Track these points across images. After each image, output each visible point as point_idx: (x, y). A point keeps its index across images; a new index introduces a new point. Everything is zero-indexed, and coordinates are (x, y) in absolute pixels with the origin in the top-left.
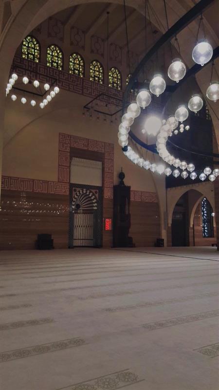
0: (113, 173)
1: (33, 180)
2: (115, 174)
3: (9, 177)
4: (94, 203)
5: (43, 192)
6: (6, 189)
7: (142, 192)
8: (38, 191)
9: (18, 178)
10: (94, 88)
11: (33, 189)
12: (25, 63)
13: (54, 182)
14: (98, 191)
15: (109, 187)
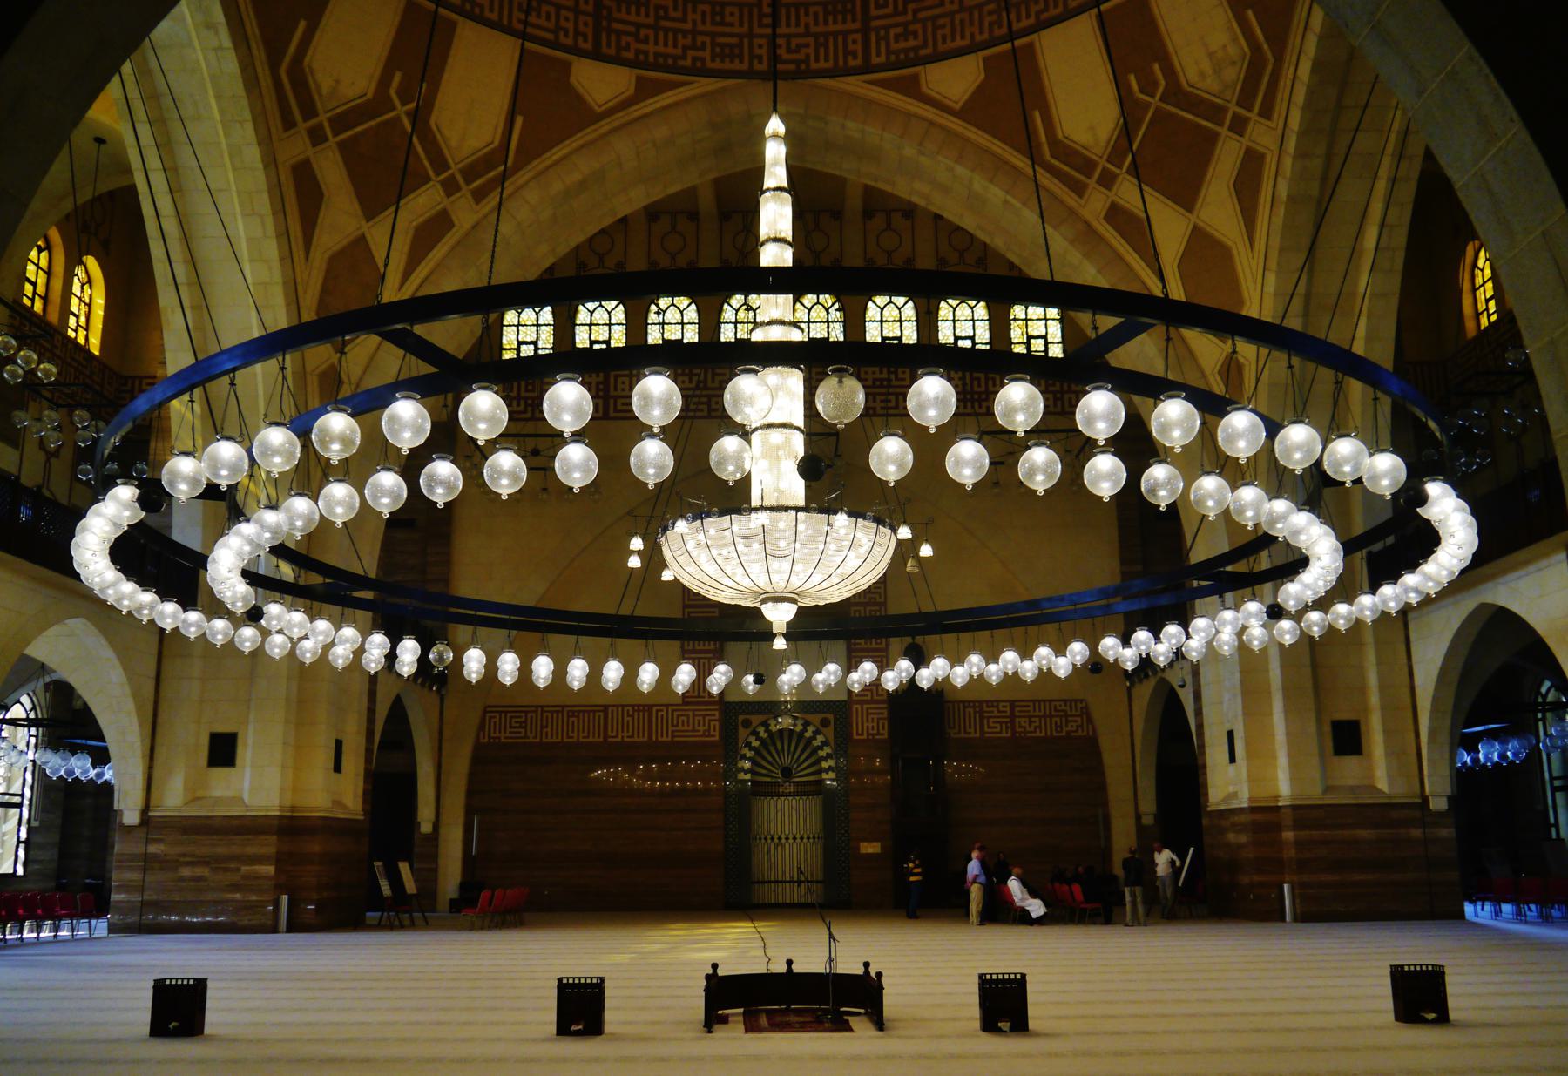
1: (606, 707)
4: (825, 759)
7: (1013, 704)
9: (563, 707)
11: (606, 736)
14: (831, 717)
15: (872, 701)
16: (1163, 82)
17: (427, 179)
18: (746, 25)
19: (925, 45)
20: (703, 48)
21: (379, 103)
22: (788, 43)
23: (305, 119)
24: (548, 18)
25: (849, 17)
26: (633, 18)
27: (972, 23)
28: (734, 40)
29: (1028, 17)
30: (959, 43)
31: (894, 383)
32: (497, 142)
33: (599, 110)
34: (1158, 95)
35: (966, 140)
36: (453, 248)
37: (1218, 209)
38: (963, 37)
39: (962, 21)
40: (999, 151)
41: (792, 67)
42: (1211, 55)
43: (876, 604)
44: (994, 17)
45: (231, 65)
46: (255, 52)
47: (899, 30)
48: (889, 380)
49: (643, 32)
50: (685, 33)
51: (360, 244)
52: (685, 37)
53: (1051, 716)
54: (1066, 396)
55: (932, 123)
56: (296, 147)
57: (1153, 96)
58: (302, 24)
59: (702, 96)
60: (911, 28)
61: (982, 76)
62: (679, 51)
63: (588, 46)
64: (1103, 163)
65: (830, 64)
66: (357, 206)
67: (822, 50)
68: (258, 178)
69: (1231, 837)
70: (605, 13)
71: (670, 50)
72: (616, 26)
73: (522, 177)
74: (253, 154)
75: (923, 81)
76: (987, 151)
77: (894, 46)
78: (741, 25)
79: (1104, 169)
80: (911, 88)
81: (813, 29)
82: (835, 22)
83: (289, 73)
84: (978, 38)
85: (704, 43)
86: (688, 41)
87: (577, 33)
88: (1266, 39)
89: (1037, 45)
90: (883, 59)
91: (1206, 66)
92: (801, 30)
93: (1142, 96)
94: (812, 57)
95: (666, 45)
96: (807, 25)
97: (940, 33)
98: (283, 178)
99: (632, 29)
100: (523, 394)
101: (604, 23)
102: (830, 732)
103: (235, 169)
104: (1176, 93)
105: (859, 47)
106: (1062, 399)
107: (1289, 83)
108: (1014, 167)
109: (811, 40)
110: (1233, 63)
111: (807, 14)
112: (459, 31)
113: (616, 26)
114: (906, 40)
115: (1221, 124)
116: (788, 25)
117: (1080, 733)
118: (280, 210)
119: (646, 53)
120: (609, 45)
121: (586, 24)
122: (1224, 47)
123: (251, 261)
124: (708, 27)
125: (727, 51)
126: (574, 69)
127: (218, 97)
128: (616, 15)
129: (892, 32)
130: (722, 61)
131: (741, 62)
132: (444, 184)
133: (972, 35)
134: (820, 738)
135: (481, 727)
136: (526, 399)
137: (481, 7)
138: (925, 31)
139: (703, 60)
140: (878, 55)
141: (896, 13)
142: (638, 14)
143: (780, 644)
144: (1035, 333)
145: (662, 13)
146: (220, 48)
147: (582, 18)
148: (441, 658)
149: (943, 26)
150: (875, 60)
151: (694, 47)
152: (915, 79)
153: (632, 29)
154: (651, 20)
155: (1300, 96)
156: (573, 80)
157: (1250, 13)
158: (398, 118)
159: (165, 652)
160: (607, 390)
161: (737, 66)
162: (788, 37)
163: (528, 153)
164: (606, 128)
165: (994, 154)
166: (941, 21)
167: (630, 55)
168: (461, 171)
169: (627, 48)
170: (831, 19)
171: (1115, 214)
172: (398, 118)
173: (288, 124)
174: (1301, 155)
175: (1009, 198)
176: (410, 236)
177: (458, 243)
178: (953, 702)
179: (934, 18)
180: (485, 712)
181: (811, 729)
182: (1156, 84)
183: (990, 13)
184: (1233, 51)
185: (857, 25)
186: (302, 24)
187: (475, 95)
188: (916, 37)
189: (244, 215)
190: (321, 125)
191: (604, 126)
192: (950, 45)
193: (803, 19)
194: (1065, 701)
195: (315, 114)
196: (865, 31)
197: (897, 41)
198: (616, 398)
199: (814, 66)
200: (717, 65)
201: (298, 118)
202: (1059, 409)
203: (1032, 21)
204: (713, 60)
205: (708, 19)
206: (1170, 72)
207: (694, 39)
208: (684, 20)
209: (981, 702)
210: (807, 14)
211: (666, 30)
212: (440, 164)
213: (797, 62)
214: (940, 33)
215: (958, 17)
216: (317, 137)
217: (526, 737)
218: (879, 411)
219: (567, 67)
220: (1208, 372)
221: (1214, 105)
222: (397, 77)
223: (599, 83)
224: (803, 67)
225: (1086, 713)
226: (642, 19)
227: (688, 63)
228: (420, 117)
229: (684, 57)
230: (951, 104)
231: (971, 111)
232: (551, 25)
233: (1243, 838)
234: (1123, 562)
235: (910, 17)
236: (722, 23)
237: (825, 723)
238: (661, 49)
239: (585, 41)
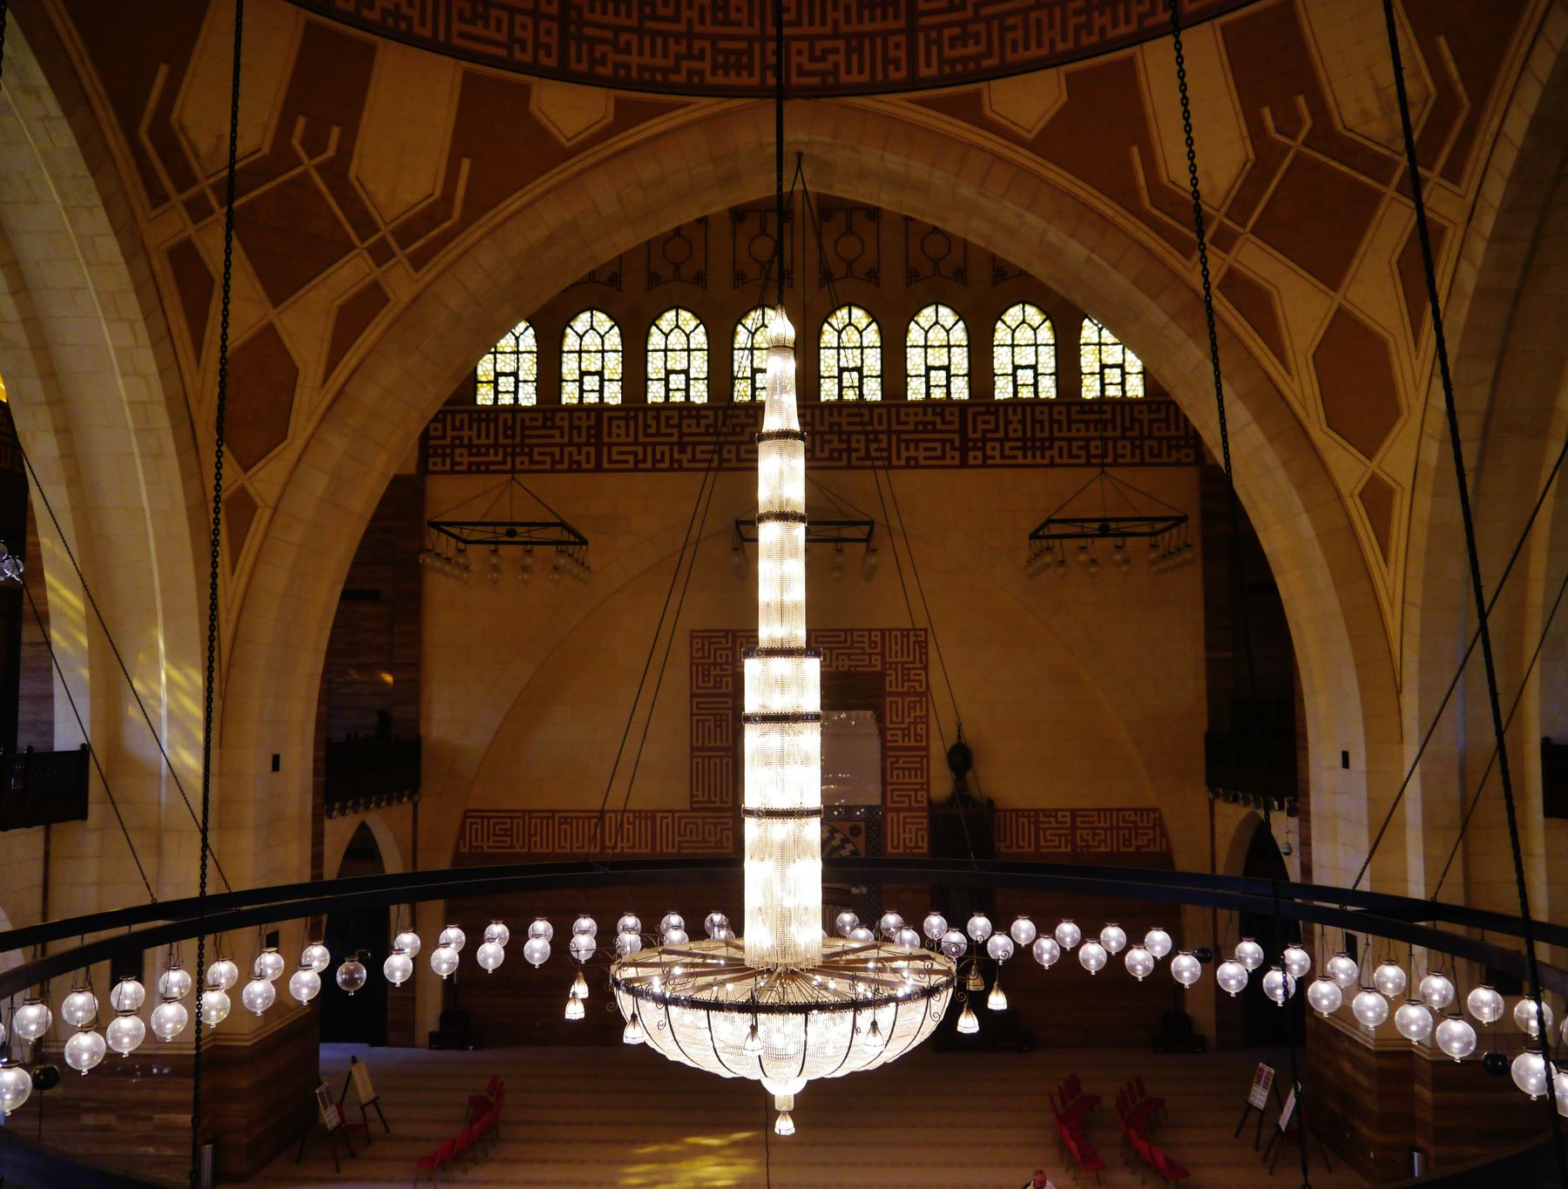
0: (927, 748)
2: (938, 751)
3: (524, 812)
5: (637, 850)
6: (518, 850)
7: (1074, 813)
8: (618, 850)
10: (826, 428)
11: (603, 847)
12: (558, 423)
13: (673, 812)
15: (910, 809)
16: (1308, 123)
17: (353, 247)
18: (757, 22)
19: (989, 55)
20: (701, 57)
21: (280, 156)
22: (812, 49)
23: (180, 190)
24: (499, 29)
26: (610, 18)
27: (1052, 26)
28: (742, 45)
29: (1127, 22)
30: (1034, 52)
31: (939, 426)
32: (437, 194)
33: (568, 145)
34: (1301, 137)
35: (1042, 180)
36: (390, 327)
37: (1374, 291)
38: (1040, 45)
39: (1039, 22)
40: (1083, 195)
41: (815, 81)
43: (916, 694)
44: (1082, 19)
45: (65, 138)
46: (101, 114)
47: (957, 31)
48: (934, 423)
49: (624, 37)
50: (678, 37)
51: (268, 336)
52: (677, 42)
53: (1119, 828)
54: (1147, 443)
55: (997, 157)
56: (171, 226)
57: (1293, 137)
58: (163, 70)
59: (699, 122)
60: (973, 28)
61: (1065, 97)
62: (670, 62)
63: (552, 62)
64: (1220, 217)
65: (865, 78)
66: (258, 286)
67: (855, 57)
68: (120, 276)
69: (1347, 1066)
70: (573, 15)
71: (659, 61)
72: (589, 31)
73: (476, 232)
74: (110, 246)
75: (986, 101)
76: (1068, 193)
77: (948, 53)
78: (751, 24)
79: (1221, 224)
80: (970, 110)
81: (844, 29)
82: (872, 19)
83: (152, 135)
84: (1060, 47)
85: (702, 50)
86: (682, 49)
87: (537, 45)
88: (1461, 74)
89: (1139, 57)
90: (933, 71)
92: (828, 29)
93: (1279, 137)
94: (842, 70)
95: (653, 54)
96: (835, 22)
98: (157, 268)
99: (609, 35)
100: (501, 441)
101: (573, 29)
102: (860, 842)
103: (88, 264)
104: (1326, 135)
105: (902, 54)
106: (1141, 447)
107: (1489, 138)
108: (1101, 215)
109: (840, 44)
112: (379, 56)
113: (589, 31)
114: (965, 46)
115: (1386, 183)
116: (811, 23)
117: (1152, 849)
118: (153, 310)
119: (627, 67)
120: (579, 60)
121: (549, 32)
123: (123, 375)
124: (710, 28)
125: (733, 59)
126: (535, 91)
127: (56, 178)
128: (587, 15)
129: (947, 33)
130: (727, 74)
131: (751, 75)
132: (370, 250)
133: (1052, 43)
134: (849, 847)
135: (461, 835)
136: (505, 447)
137: (408, 20)
138: (989, 36)
139: (701, 73)
140: (928, 65)
143: (785, 1126)
144: (1110, 362)
146: (48, 117)
147: (544, 24)
148: (351, 981)
149: (1014, 28)
150: (924, 72)
151: (689, 56)
152: (977, 96)
153: (609, 35)
154: (633, 22)
155: (1506, 160)
156: (533, 108)
158: (306, 174)
159: (53, 852)
160: (599, 436)
161: (745, 80)
162: (811, 39)
163: (477, 206)
164: (576, 169)
165: (1075, 198)
166: (1010, 21)
167: (606, 71)
168: (393, 233)
169: (603, 62)
170: (866, 13)
171: (1235, 284)
172: (306, 174)
173: (157, 198)
174: (1497, 238)
175: (1094, 256)
176: (332, 319)
177: (397, 319)
178: (1004, 811)
179: (1001, 17)
180: (465, 817)
181: (838, 836)
182: (1299, 122)
183: (1077, 13)
185: (901, 24)
186: (163, 70)
187: (407, 130)
188: (977, 43)
189: (108, 320)
190: (202, 195)
191: (573, 166)
192: (1023, 55)
193: (830, 15)
194: (1135, 810)
195: (194, 181)
196: (911, 31)
197: (952, 47)
198: (610, 445)
199: (845, 79)
200: (720, 80)
201: (169, 186)
202: (1137, 459)
203: (1133, 27)
204: (714, 74)
205: (708, 19)
206: (1320, 109)
207: (690, 47)
208: (676, 19)
209: (1037, 811)
211: (654, 34)
212: (366, 225)
213: (823, 74)
214: (1009, 36)
215: (1033, 15)
216: (198, 210)
217: (512, 847)
218: (922, 462)
219: (525, 90)
220: (1345, 491)
221: (1377, 155)
222: (301, 122)
223: (568, 109)
224: (830, 80)
225: (1160, 825)
226: (622, 21)
227: (682, 78)
228: (337, 172)
229: (676, 70)
230: (1025, 134)
231: (1046, 143)
232: (503, 37)
233: (1364, 1080)
234: (1210, 647)
236: (726, 22)
237: (855, 831)
238: (647, 60)
239: (548, 55)
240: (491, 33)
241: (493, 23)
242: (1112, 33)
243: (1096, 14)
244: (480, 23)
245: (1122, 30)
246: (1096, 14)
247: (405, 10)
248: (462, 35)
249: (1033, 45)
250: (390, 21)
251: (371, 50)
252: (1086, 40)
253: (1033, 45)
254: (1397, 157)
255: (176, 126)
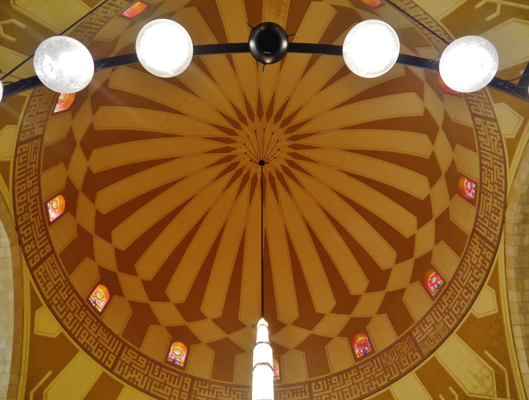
25: (303, 394)
26: (206, 395)
27: (359, 388)
38: (356, 394)
39: (355, 389)
42: (475, 376)
44: (369, 384)
58: (50, 373)
70: (194, 392)
82: (297, 396)
84: (363, 393)
88: (498, 361)
91: (475, 382)
97: (345, 395)
101: (193, 396)
107: (519, 379)
110: (488, 377)
111: (284, 394)
112: (124, 389)
122: (480, 371)
128: (198, 393)
133: (360, 393)
141: (324, 390)
142: (209, 394)
145: (219, 394)
147: (183, 393)
149: (347, 392)
157: (486, 352)
166: (345, 390)
179: (342, 390)
184: (486, 372)
186: (50, 373)
203: (386, 381)
205: (240, 397)
206: (458, 389)
210: (284, 394)
215: (352, 388)
235: (331, 391)
240: (164, 392)
241: (165, 390)
242: (380, 385)
243: (373, 382)
244: (161, 389)
245: (383, 383)
246: (373, 382)
247: (137, 379)
248: (154, 390)
249: (354, 394)
250: (131, 381)
251: (122, 386)
252: (372, 389)
253: (354, 394)
254: (493, 398)
255: (44, 394)
